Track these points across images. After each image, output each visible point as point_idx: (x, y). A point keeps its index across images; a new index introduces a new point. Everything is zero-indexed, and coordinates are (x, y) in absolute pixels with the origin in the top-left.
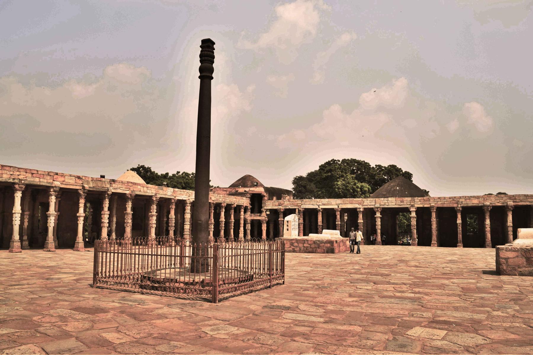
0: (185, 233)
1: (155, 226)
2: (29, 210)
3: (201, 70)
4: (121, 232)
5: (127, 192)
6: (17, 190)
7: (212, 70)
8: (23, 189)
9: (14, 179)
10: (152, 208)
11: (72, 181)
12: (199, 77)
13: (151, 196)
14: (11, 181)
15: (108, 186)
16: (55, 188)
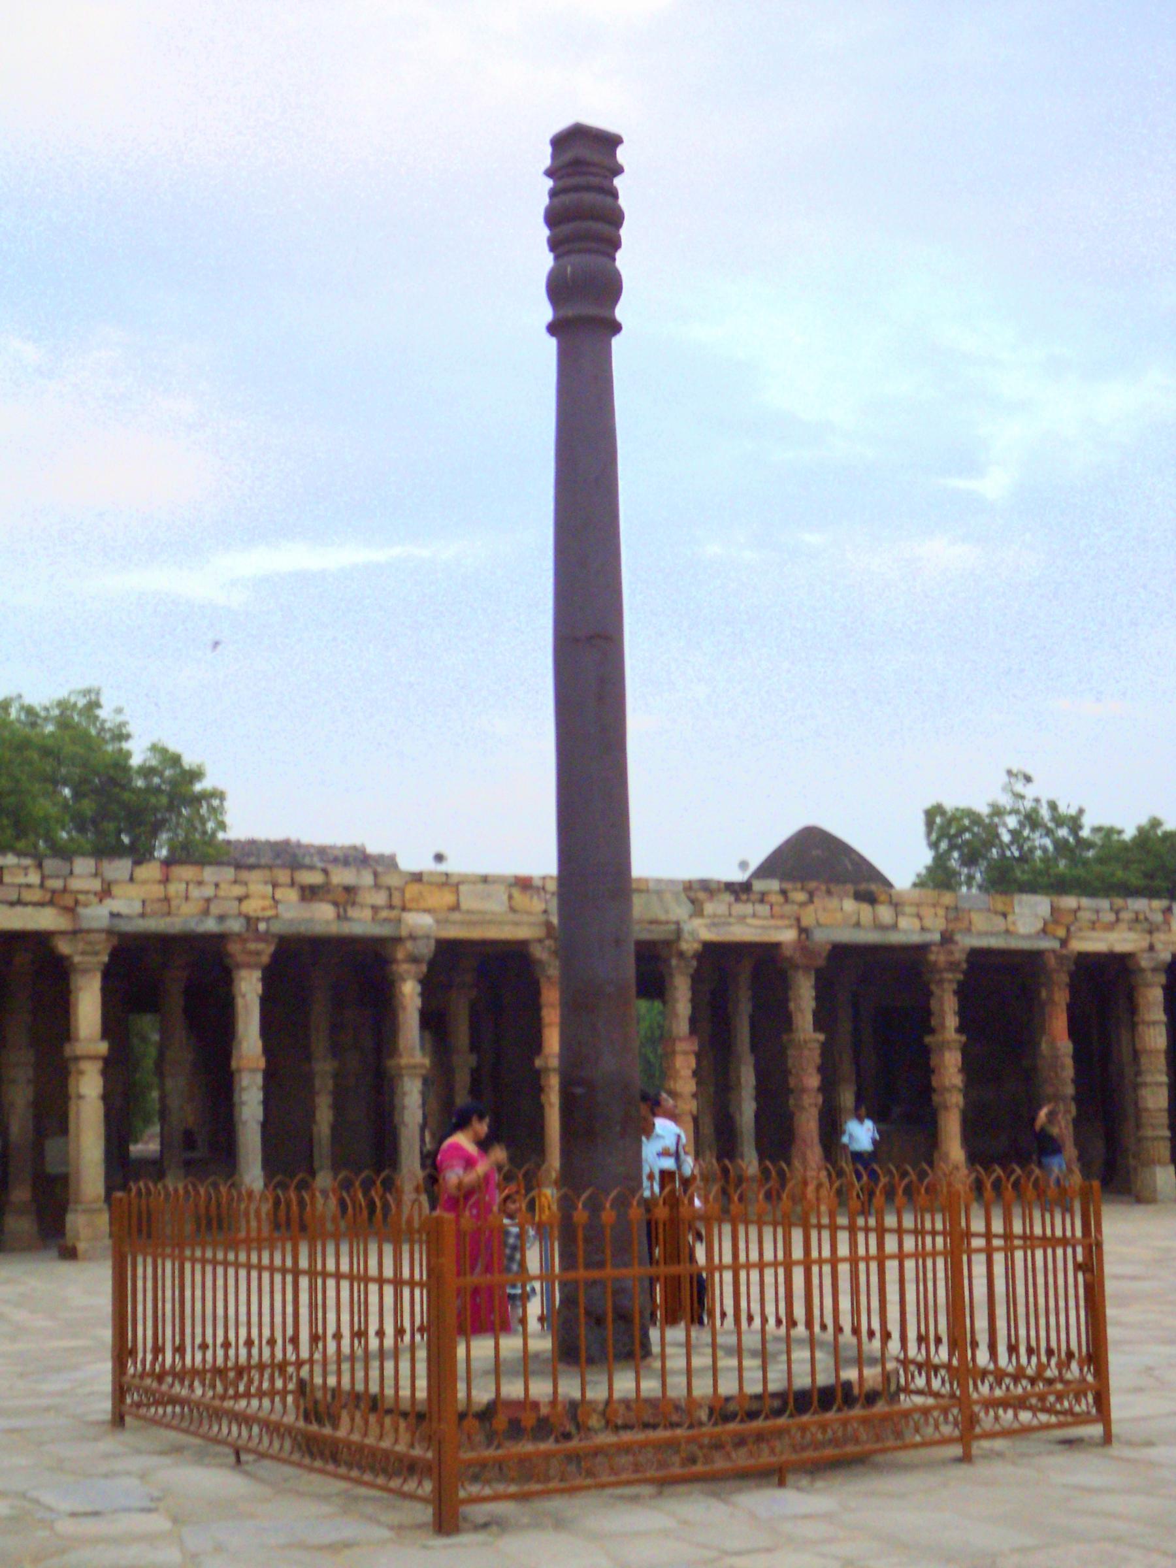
0: (1149, 1133)
1: (956, 1100)
2: (336, 1050)
3: (558, 289)
4: (211, 1147)
5: (787, 936)
6: (239, 966)
7: (611, 288)
8: (265, 959)
9: (221, 918)
10: (934, 1005)
11: (496, 904)
12: (552, 329)
13: (922, 949)
14: (210, 925)
15: (679, 911)
16: (409, 945)
